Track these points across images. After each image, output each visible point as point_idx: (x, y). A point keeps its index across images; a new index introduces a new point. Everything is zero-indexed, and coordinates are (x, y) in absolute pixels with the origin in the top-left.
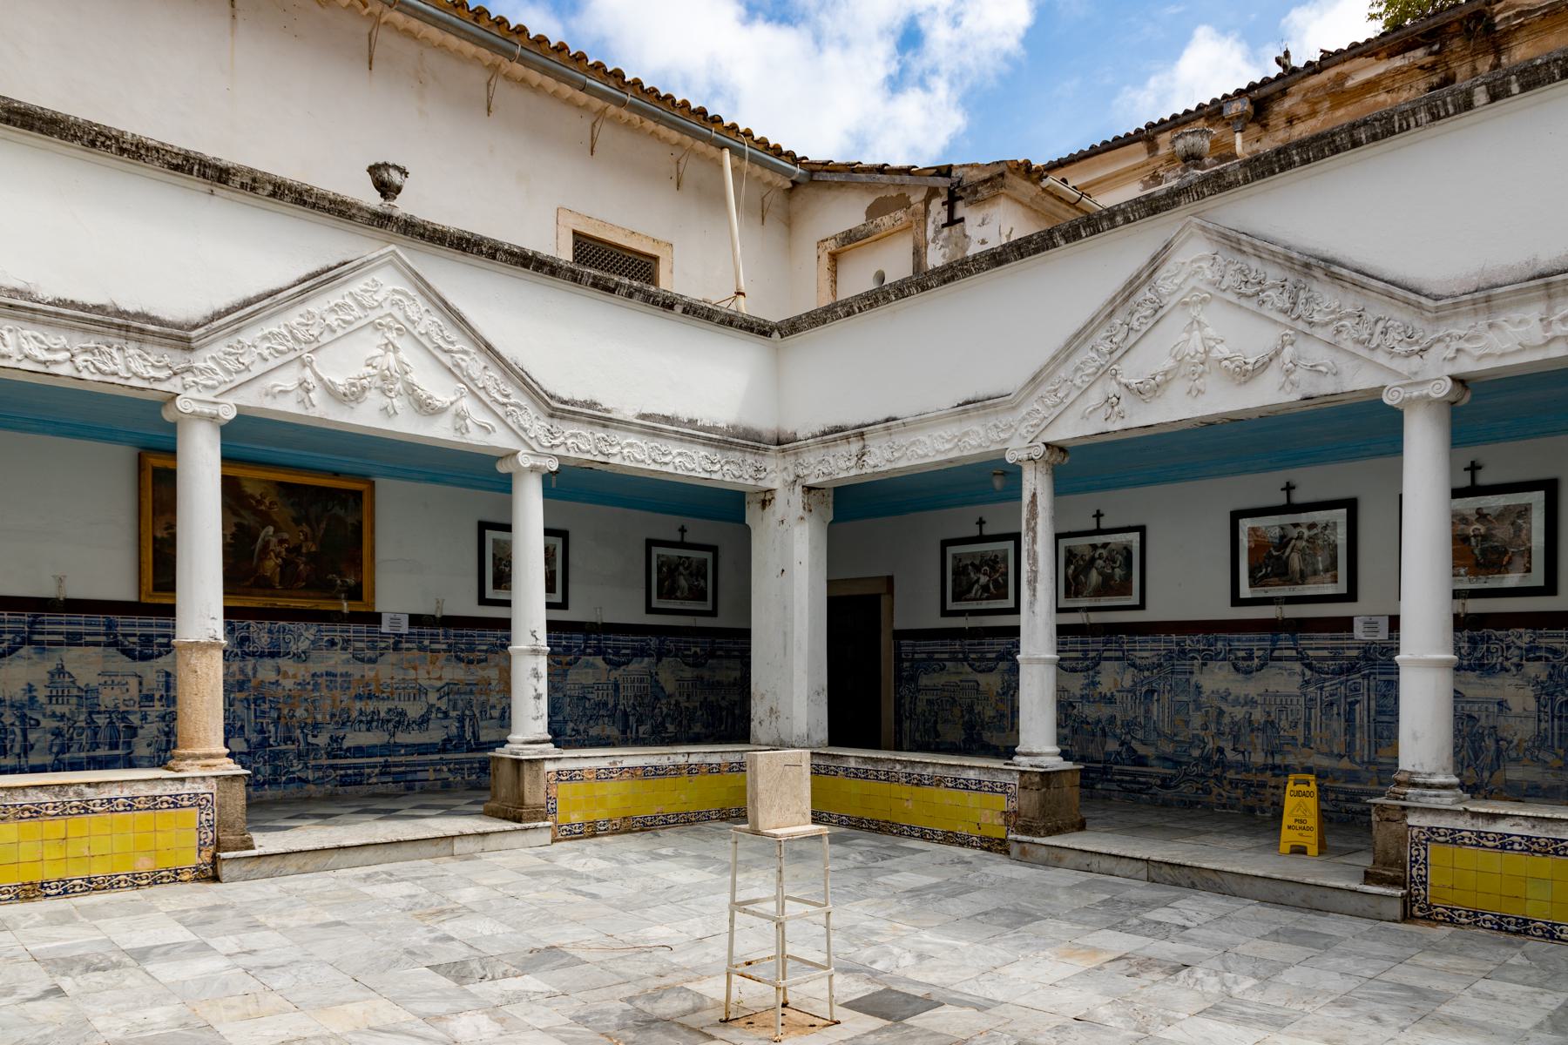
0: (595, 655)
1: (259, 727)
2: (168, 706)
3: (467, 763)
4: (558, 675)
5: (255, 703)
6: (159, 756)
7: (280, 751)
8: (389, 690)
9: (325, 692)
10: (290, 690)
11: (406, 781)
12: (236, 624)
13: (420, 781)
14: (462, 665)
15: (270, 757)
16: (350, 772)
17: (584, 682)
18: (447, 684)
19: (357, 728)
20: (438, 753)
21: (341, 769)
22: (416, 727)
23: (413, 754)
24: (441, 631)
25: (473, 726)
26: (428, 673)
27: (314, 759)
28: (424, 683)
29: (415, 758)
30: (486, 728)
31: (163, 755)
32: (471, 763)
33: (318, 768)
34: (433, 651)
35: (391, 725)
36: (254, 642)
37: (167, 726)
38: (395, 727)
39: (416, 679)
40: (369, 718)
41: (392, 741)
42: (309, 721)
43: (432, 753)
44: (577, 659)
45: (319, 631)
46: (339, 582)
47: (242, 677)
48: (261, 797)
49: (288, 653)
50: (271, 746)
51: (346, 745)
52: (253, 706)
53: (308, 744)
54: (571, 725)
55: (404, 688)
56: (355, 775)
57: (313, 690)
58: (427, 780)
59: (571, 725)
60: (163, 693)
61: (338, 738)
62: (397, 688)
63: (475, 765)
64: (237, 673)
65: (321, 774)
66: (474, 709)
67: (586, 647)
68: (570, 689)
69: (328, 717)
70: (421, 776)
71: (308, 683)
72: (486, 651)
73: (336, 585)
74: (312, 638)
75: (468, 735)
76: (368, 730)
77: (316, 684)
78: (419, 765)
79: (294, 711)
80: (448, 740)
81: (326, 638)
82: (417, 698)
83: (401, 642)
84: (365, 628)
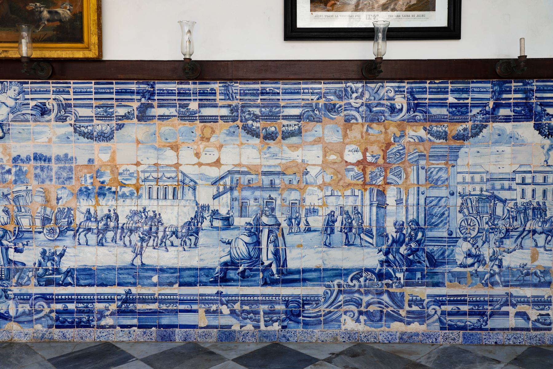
0: (516, 120)
3: (264, 303)
4: (438, 157)
8: (134, 181)
9: (33, 184)
11: (160, 326)
13: (182, 327)
14: (256, 141)
16: (71, 306)
17: (493, 169)
18: (230, 172)
19: (83, 240)
20: (214, 283)
21: (58, 301)
22: (177, 242)
23: (171, 284)
24: (217, 86)
25: (275, 243)
26: (197, 155)
27: (18, 284)
28: (191, 171)
29: (176, 290)
30: (300, 246)
32: (271, 302)
33: (24, 298)
34: (204, 119)
35: (135, 238)
38: (142, 240)
39: (177, 165)
40: (101, 225)
41: (137, 262)
42: (10, 227)
43: (205, 284)
44: (478, 130)
45: (22, 92)
46: (45, 14)
51: (65, 265)
53: (10, 261)
54: (464, 247)
55: (157, 180)
56: (80, 312)
57: (15, 182)
58: (194, 327)
59: (465, 246)
61: (54, 254)
62: (146, 180)
63: (277, 307)
65: (27, 307)
66: (278, 214)
67: (497, 106)
68: (464, 182)
69: (38, 223)
70: (184, 319)
71: (9, 172)
72: (299, 118)
73: (41, 19)
74: (11, 103)
75: (267, 257)
76: (100, 243)
77: (20, 173)
78: (182, 302)
80: (232, 264)
81: (33, 103)
82: (180, 195)
83: (152, 106)
84: (92, 86)
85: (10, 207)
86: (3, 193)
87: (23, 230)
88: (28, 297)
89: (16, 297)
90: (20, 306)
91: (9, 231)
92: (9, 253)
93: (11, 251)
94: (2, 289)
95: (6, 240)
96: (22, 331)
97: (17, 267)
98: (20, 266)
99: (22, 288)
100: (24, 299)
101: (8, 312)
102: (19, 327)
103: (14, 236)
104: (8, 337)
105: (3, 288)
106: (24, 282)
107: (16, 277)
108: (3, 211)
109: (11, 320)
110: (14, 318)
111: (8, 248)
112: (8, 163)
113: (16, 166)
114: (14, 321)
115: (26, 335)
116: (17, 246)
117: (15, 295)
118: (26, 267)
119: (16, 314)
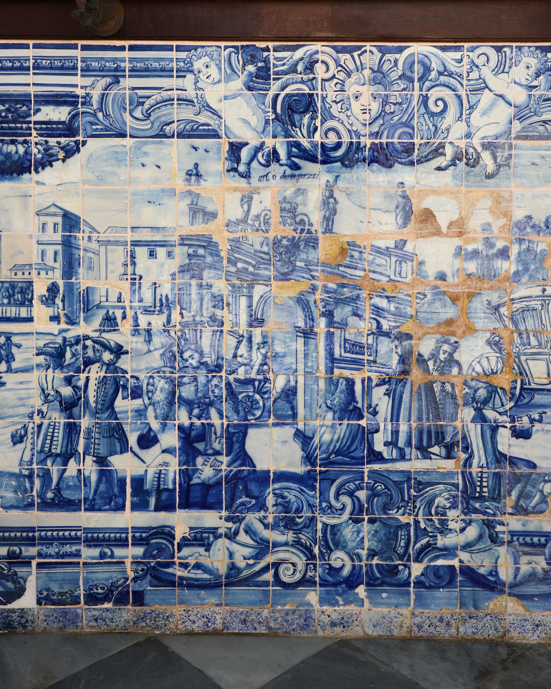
1: (339, 398)
2: (71, 322)
5: (329, 315)
6: (46, 476)
7: (407, 475)
10: (442, 277)
12: (272, 55)
15: (373, 494)
31: (55, 471)
36: (328, 116)
37: (68, 381)
47: (289, 232)
48: (343, 623)
49: (438, 151)
50: (378, 457)
52: (321, 324)
60: (57, 276)
64: (275, 217)
71: (504, 253)
79: (456, 346)
85: (505, 334)
86: (489, 303)
87: (533, 386)
88: (543, 540)
89: (515, 538)
90: (524, 559)
91: (502, 388)
92: (499, 438)
93: (504, 435)
94: (483, 520)
95: (494, 409)
96: (528, 616)
97: (517, 471)
98: (525, 470)
99: (526, 518)
100: (532, 545)
101: (497, 572)
102: (521, 608)
103: (511, 399)
104: (496, 629)
105: (485, 517)
106: (532, 504)
107: (514, 494)
108: (489, 343)
109: (502, 592)
110: (511, 587)
111: (498, 427)
112: (503, 235)
113: (520, 241)
114: (510, 594)
115: (537, 626)
116: (516, 424)
117: (513, 534)
118: (538, 471)
119: (515, 577)
